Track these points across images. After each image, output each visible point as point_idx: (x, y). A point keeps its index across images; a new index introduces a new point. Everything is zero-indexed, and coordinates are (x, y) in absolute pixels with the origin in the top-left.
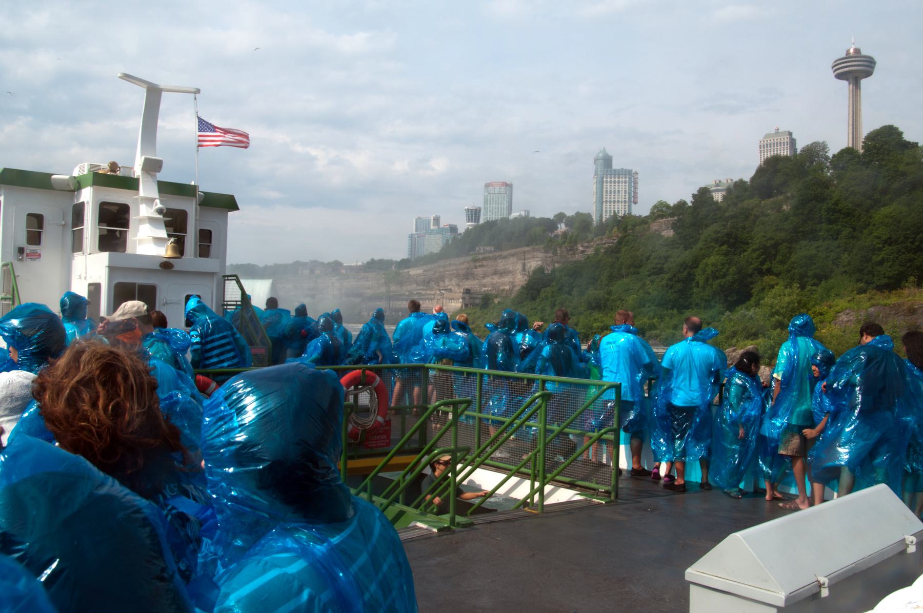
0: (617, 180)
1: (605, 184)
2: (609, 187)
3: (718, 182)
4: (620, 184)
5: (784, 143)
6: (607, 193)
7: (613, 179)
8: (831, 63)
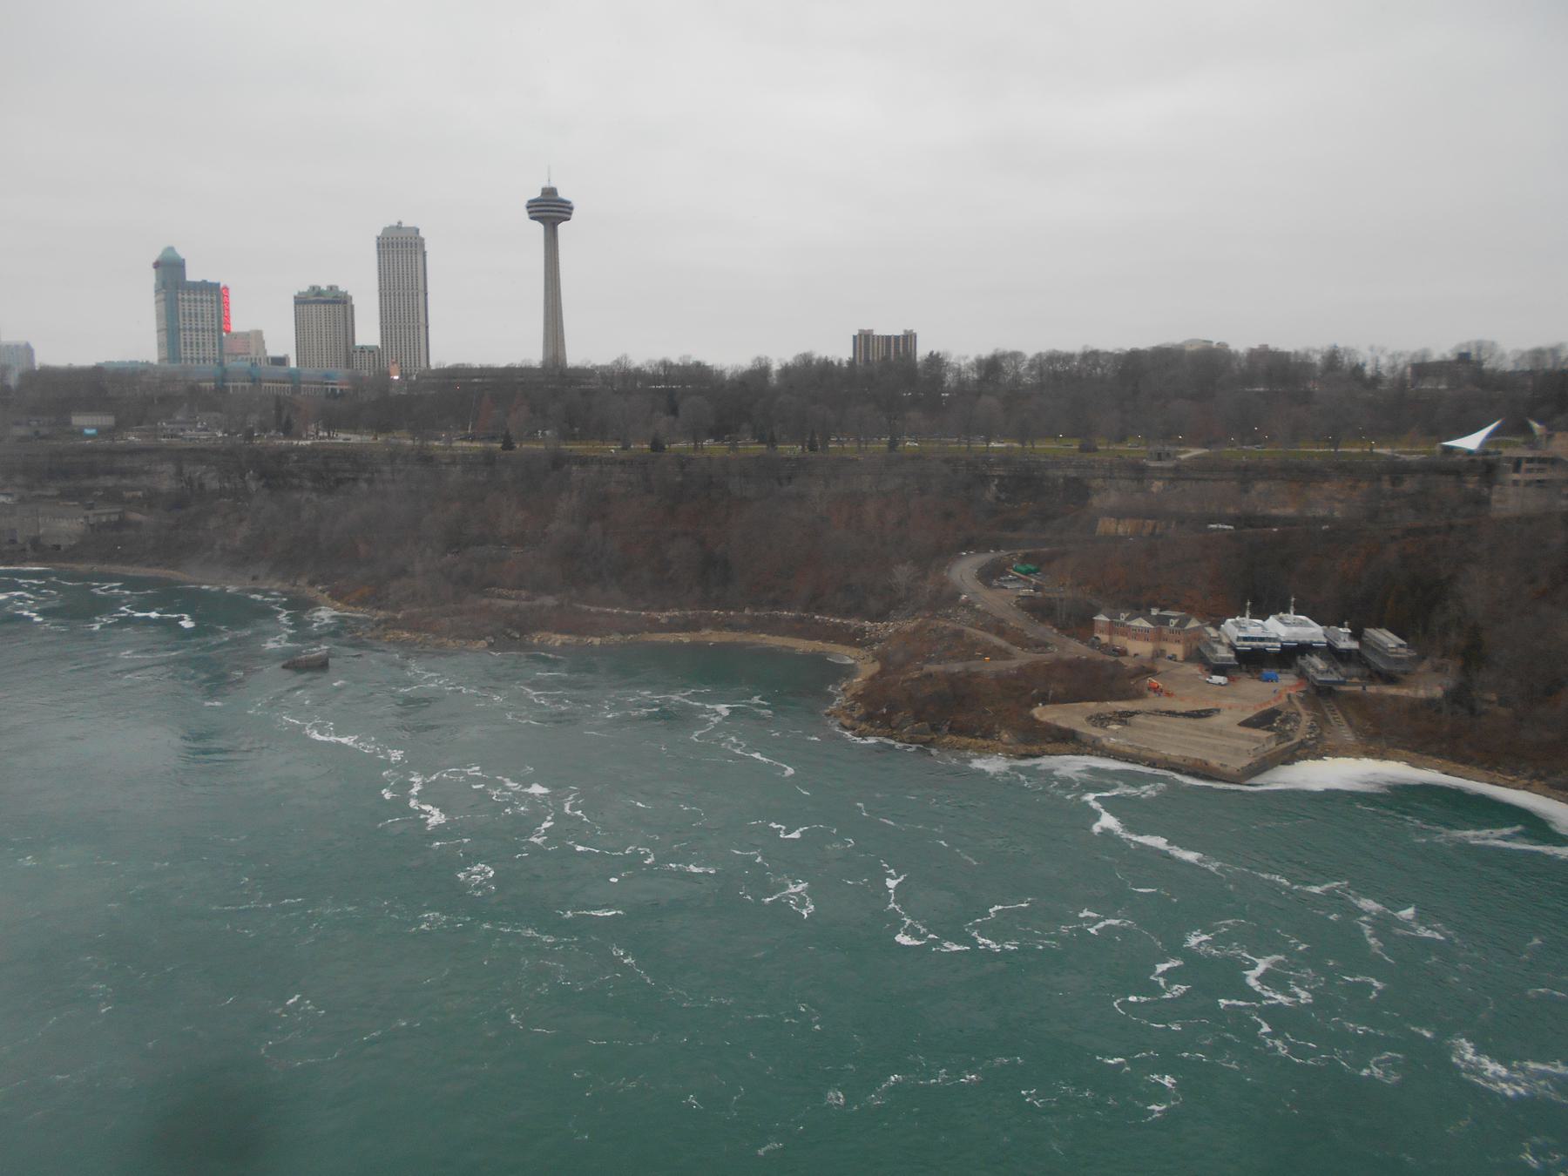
0: (198, 297)
1: (180, 303)
2: (187, 308)
3: (317, 289)
4: (205, 304)
5: (411, 244)
6: (184, 316)
7: (192, 297)
8: (525, 203)
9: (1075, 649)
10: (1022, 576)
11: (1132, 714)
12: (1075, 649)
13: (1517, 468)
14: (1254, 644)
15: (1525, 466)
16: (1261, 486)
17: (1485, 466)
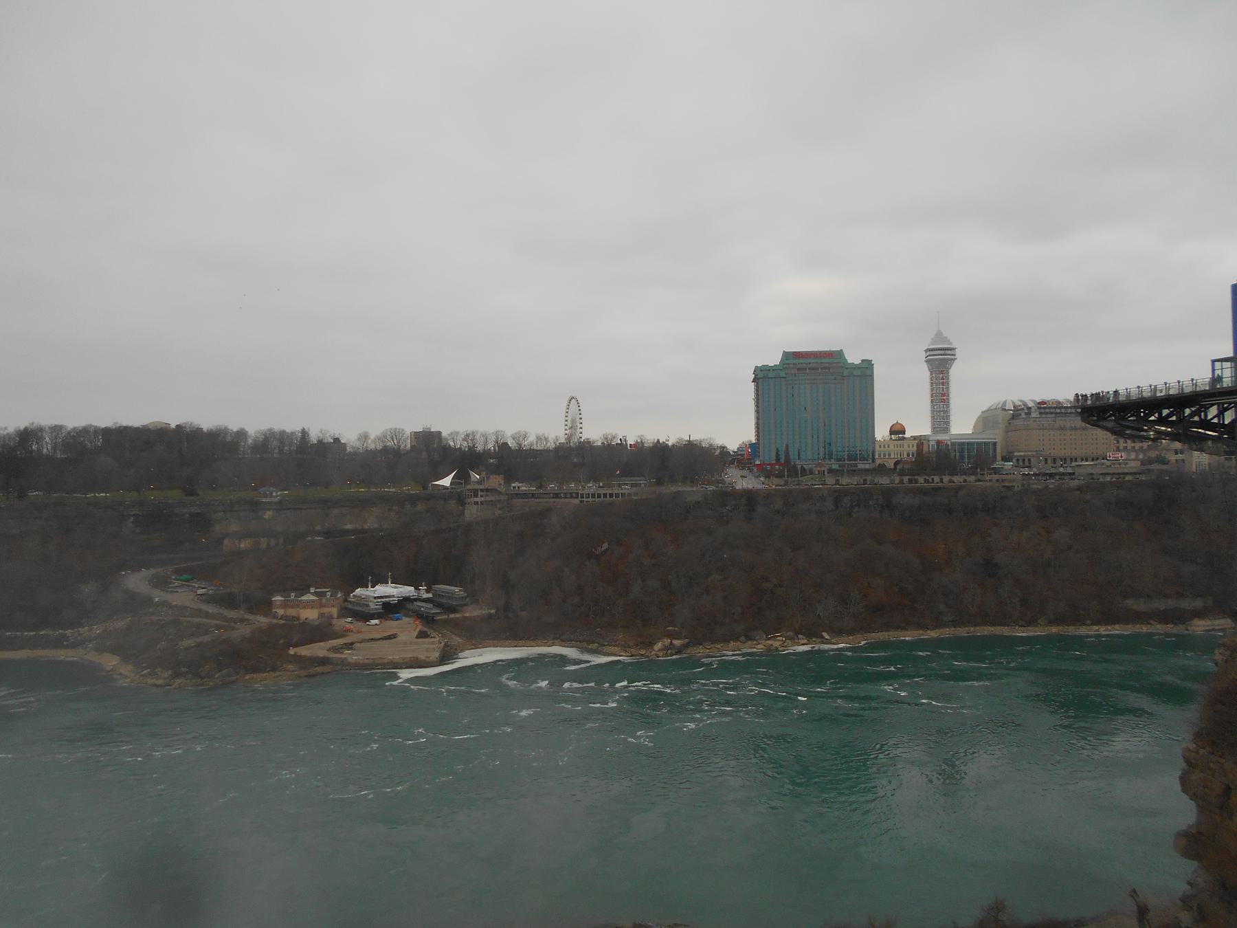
9: (262, 621)
10: (184, 583)
11: (352, 644)
12: (262, 621)
13: (476, 496)
14: (383, 600)
15: (480, 493)
16: (336, 511)
17: (456, 496)
